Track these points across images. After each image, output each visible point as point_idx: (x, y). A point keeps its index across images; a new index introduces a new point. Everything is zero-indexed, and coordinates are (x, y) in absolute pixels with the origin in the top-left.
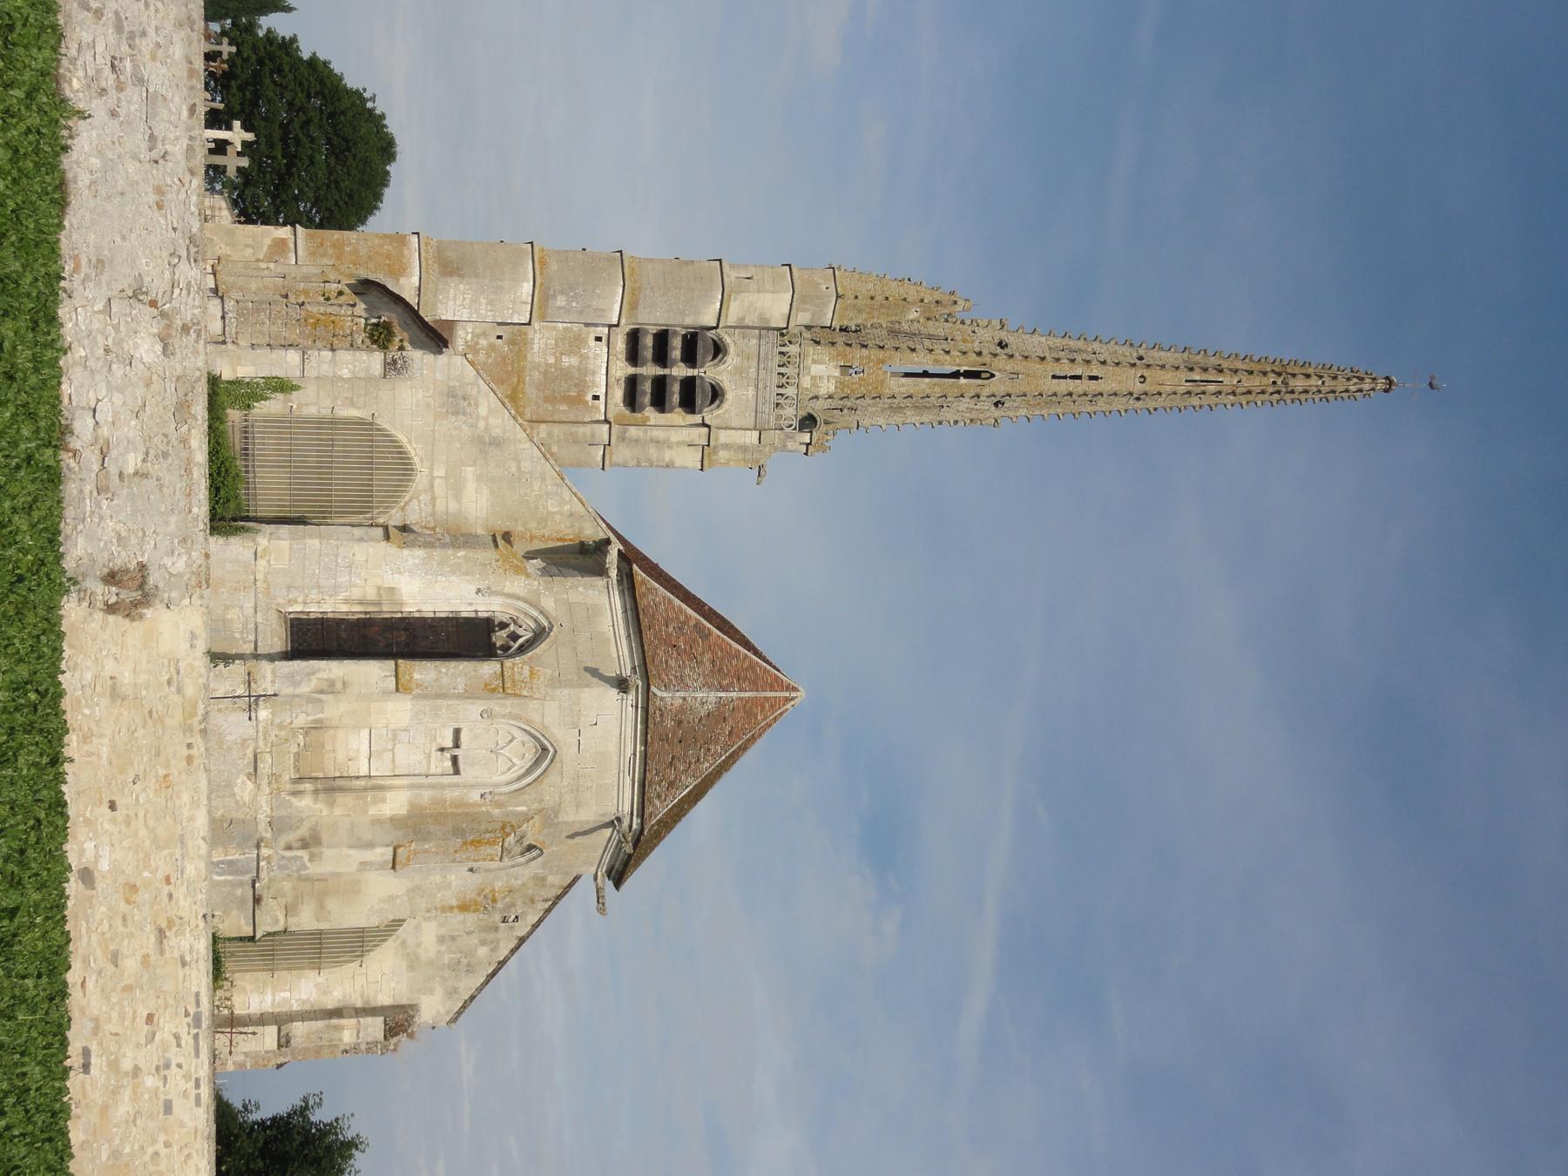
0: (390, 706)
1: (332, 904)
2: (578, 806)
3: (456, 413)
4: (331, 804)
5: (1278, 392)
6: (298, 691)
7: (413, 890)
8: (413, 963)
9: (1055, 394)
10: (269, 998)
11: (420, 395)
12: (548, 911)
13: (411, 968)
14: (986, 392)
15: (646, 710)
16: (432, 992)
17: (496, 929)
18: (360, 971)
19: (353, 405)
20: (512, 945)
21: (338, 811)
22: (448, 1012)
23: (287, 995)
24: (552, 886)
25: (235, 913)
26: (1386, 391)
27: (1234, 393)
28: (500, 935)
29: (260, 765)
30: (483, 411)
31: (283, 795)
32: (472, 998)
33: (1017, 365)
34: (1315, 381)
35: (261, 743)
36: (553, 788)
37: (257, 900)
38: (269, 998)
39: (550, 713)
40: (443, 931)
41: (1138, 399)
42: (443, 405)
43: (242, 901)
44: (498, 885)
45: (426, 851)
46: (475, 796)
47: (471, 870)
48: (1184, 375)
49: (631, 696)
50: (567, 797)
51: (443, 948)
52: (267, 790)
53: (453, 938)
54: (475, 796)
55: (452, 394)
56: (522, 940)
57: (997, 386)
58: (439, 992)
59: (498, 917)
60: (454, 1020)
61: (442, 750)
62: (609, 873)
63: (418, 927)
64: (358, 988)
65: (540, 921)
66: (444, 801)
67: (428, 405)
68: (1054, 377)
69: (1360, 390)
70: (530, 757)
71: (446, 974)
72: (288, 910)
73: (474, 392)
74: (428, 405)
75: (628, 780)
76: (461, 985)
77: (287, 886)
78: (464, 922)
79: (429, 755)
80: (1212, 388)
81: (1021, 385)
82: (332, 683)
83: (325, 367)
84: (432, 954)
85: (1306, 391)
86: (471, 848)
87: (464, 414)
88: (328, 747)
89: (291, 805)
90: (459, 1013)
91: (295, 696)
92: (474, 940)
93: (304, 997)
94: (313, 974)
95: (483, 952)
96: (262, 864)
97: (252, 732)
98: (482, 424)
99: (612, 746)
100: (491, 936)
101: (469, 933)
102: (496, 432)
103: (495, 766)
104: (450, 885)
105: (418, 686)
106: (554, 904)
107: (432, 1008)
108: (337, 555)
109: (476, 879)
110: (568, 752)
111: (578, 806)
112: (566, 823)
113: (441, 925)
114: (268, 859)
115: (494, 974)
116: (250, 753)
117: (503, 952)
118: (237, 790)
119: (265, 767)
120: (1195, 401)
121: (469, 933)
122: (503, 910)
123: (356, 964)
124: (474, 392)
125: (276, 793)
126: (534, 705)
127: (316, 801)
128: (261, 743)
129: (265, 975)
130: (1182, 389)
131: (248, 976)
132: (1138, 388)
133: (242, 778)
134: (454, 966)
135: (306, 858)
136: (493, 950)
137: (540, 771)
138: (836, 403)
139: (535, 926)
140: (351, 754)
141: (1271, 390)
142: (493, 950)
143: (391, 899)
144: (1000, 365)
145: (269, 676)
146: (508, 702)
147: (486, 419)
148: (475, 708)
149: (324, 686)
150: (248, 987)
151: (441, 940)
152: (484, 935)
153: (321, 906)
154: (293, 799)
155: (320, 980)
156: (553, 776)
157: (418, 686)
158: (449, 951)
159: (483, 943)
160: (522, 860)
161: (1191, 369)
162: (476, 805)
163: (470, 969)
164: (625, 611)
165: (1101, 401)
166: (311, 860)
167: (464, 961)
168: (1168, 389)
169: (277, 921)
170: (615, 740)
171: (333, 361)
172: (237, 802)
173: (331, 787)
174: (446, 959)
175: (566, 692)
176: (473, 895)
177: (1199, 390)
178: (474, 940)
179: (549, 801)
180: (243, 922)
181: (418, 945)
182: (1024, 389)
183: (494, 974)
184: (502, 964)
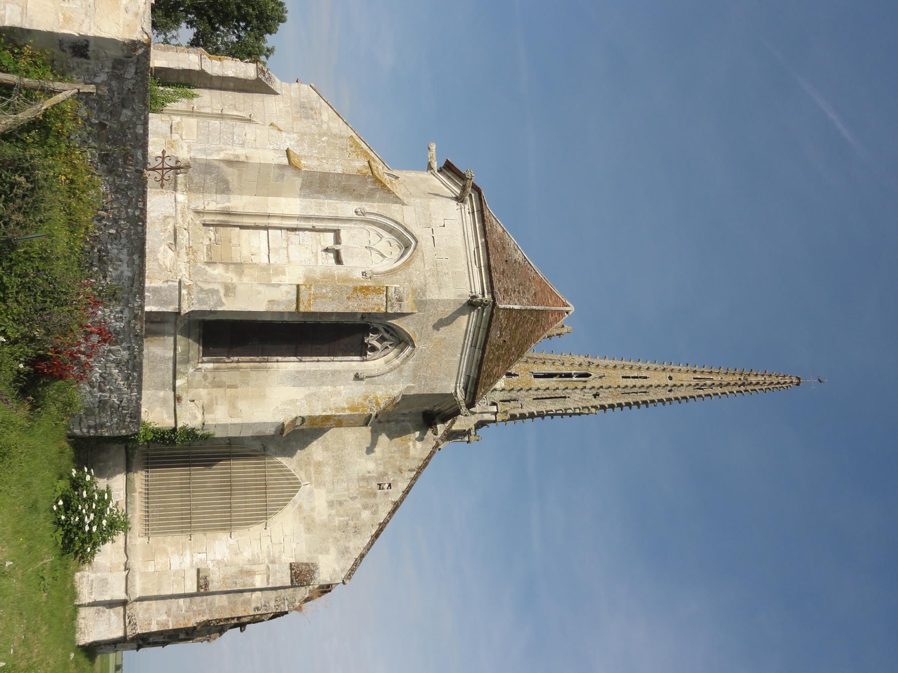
0: (283, 200)
1: (242, 405)
2: (440, 288)
3: (307, 118)
4: (240, 273)
5: (743, 384)
6: (208, 158)
7: (309, 395)
8: (310, 525)
9: (626, 386)
10: (188, 559)
11: (282, 105)
12: (415, 479)
13: (308, 530)
14: (588, 386)
15: (481, 212)
16: (327, 551)
17: (375, 495)
18: (265, 533)
19: (235, 108)
20: (389, 508)
21: (245, 280)
22: (342, 570)
23: (203, 556)
24: (414, 458)
25: (158, 409)
26: (798, 384)
27: (721, 385)
28: (378, 500)
29: (180, 237)
30: (325, 117)
31: (199, 265)
32: (362, 556)
33: (601, 372)
34: (760, 378)
35: (180, 219)
36: (419, 272)
37: (177, 399)
38: (188, 559)
39: (407, 215)
40: (331, 497)
41: (670, 391)
42: (298, 112)
43: (165, 401)
44: (379, 393)
45: (324, 296)
46: (358, 275)
47: (357, 377)
48: (692, 376)
49: (468, 206)
50: (431, 280)
51: (333, 512)
52: (186, 259)
53: (341, 503)
54: (358, 275)
55: (303, 106)
56: (397, 506)
57: (591, 382)
58: (333, 551)
59: (374, 485)
60: (349, 576)
61: (327, 250)
62: (465, 388)
63: (311, 493)
64: (264, 548)
65: (410, 487)
66: (333, 276)
67: (287, 112)
68: (623, 377)
69: (785, 383)
70: (397, 252)
71: (338, 534)
72: (204, 410)
73: (318, 106)
74: (287, 112)
75: (476, 269)
76: (351, 545)
77: (203, 392)
78: (348, 489)
79: (316, 255)
80: (709, 382)
81: (605, 383)
82: (238, 156)
83: (217, 69)
84: (325, 517)
85: (758, 383)
86: (361, 295)
87: (313, 119)
88: (234, 242)
89: (206, 272)
90: (352, 571)
91: (208, 168)
92: (358, 504)
93: (219, 557)
94: (223, 536)
95: (366, 515)
96: (184, 292)
97: (171, 211)
98: (325, 126)
99: (459, 243)
100: (371, 501)
101: (353, 499)
102: (335, 131)
103: (368, 255)
104: (340, 393)
105: (305, 167)
106: (418, 473)
107: (328, 568)
108: (233, 134)
109: (360, 388)
110: (425, 243)
111: (440, 288)
112: (432, 302)
113: (329, 492)
114: (189, 287)
115: (377, 535)
116: (170, 228)
117: (383, 516)
118: (159, 256)
119: (183, 238)
120: (701, 392)
121: (353, 499)
122: (377, 479)
123: (262, 526)
124: (318, 106)
125: (192, 263)
126: (396, 207)
127: (227, 270)
128: (180, 219)
129: (183, 538)
130: (693, 383)
131: (169, 539)
132: (670, 383)
133: (163, 247)
134: (344, 528)
135: (222, 292)
136: (375, 513)
137: (406, 257)
138: (506, 395)
139: (406, 492)
140: (253, 250)
141: (740, 383)
142: (375, 513)
143: (293, 402)
144: (592, 370)
145: (185, 148)
146: (375, 204)
147: (328, 123)
148: (348, 208)
149: (232, 158)
150: (170, 549)
151: (331, 504)
152: (365, 500)
153: (233, 405)
154: (209, 269)
155: (231, 541)
156: (417, 263)
157: (305, 167)
158: (339, 515)
159: (365, 507)
160: (397, 362)
161: (695, 372)
162: (358, 280)
163: (357, 531)
164: (449, 178)
165: (651, 390)
166: (226, 295)
167: (352, 523)
168: (685, 383)
169: (195, 418)
170: (461, 238)
171: (222, 66)
172: (160, 265)
173: (239, 267)
174: (337, 521)
175: (418, 200)
176: (360, 400)
177: (702, 383)
178: (358, 504)
179: (418, 281)
180: (165, 416)
181: (313, 509)
182: (609, 384)
183: (377, 535)
184: (382, 526)
